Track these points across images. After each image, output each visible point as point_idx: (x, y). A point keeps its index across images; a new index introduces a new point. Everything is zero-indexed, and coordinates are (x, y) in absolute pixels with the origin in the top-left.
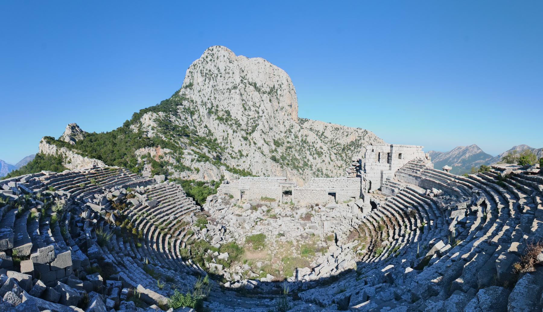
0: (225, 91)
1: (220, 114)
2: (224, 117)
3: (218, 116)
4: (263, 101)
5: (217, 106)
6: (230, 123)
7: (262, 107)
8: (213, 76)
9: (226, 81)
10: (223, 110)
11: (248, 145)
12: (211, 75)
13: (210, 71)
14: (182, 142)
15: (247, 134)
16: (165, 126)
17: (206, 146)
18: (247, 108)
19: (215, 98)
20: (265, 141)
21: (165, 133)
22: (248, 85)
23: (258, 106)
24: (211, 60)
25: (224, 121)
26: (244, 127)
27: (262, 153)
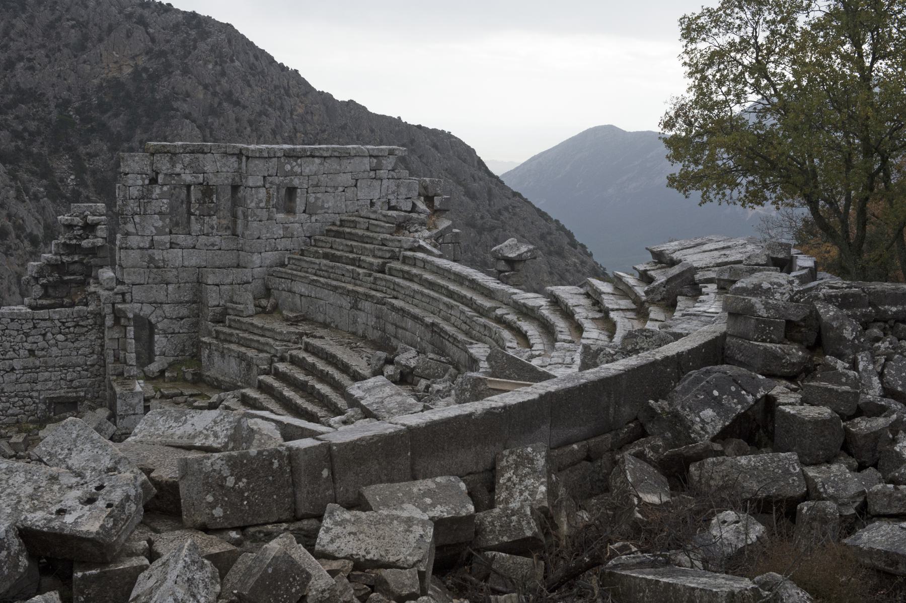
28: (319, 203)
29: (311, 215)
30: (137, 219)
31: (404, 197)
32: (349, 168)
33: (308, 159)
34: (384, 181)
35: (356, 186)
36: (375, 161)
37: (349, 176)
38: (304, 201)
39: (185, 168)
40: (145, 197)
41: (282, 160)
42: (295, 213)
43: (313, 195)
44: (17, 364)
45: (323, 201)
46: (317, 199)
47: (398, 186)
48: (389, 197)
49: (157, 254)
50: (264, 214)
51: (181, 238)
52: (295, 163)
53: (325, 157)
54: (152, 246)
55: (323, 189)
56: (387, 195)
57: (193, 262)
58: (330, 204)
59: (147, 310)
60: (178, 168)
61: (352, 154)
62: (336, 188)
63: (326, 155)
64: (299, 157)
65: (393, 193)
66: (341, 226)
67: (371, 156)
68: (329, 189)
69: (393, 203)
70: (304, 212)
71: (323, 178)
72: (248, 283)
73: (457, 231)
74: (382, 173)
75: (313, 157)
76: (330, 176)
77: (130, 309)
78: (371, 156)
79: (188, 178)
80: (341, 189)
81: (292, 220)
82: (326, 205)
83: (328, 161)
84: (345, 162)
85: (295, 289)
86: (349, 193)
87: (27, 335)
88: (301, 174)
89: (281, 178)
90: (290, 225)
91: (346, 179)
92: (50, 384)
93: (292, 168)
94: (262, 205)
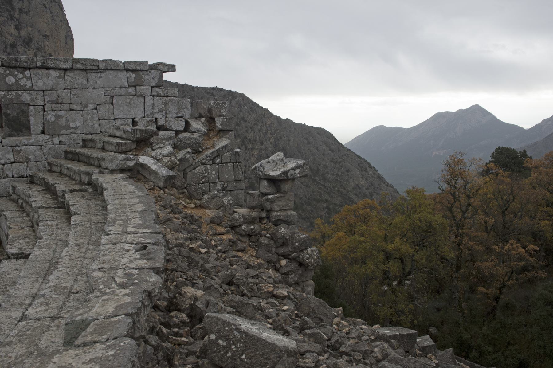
28: (62, 122)
29: (52, 136)
31: (174, 116)
32: (100, 83)
33: (39, 71)
34: (149, 99)
35: (112, 104)
36: (133, 75)
37: (101, 91)
38: (40, 120)
42: (30, 134)
43: (53, 113)
45: (67, 120)
46: (58, 117)
47: (166, 104)
48: (156, 116)
52: (20, 76)
53: (65, 70)
55: (66, 107)
56: (153, 113)
58: (78, 124)
61: (102, 67)
62: (85, 105)
63: (63, 66)
64: (26, 69)
65: (160, 111)
66: (84, 146)
67: (127, 70)
68: (75, 107)
69: (161, 122)
70: (43, 132)
71: (63, 94)
73: (238, 150)
74: (145, 89)
75: (48, 68)
76: (75, 92)
78: (127, 70)
80: (91, 107)
81: (26, 142)
82: (72, 125)
83: (71, 74)
84: (93, 76)
86: (103, 111)
88: (32, 88)
90: (23, 148)
91: (99, 95)
93: (18, 81)
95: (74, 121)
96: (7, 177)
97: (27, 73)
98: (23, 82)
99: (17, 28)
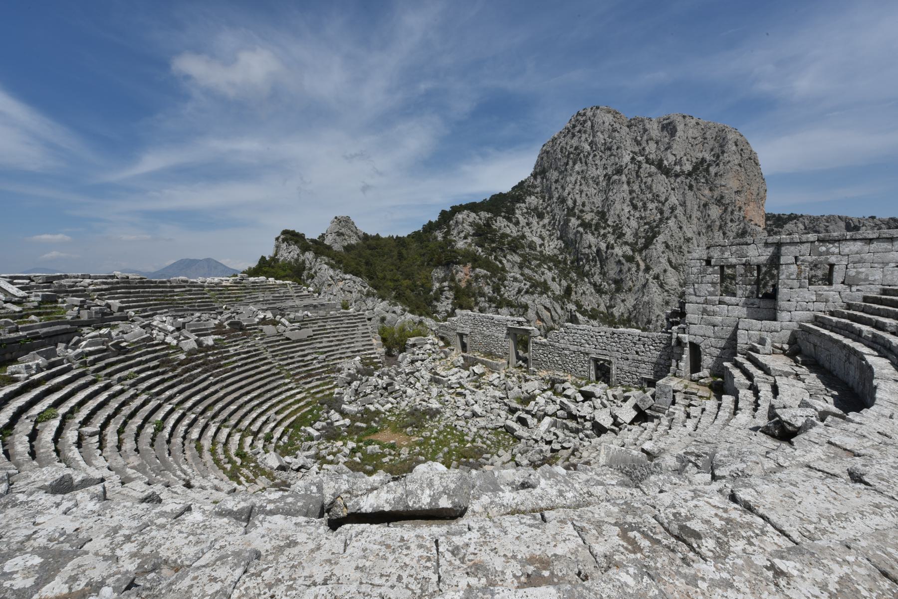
0: (601, 179)
1: (588, 217)
2: (594, 222)
3: (583, 220)
4: (673, 189)
5: (584, 205)
6: (602, 232)
7: (673, 200)
8: (582, 155)
9: (604, 161)
10: (592, 211)
11: (634, 269)
12: (579, 154)
13: (576, 148)
14: (508, 261)
15: (633, 251)
16: (483, 233)
17: (550, 269)
18: (640, 204)
19: (581, 192)
20: (670, 262)
21: (481, 246)
22: (644, 165)
23: (663, 199)
24: (580, 131)
25: (593, 228)
26: (629, 237)
27: (661, 286)
29: (850, 286)
30: (696, 286)
39: (732, 254)
40: (703, 272)
41: (816, 243)
44: (630, 357)
46: (858, 273)
49: (710, 308)
50: (796, 283)
51: (727, 299)
54: (706, 302)
57: (736, 314)
58: (877, 277)
59: (698, 340)
60: (726, 256)
71: (866, 256)
72: (777, 332)
77: (686, 338)
79: (733, 260)
85: (811, 340)
87: (635, 344)
89: (814, 257)
92: (645, 371)
94: (794, 277)
95: (873, 276)
96: (809, 310)
97: (836, 244)
98: (831, 250)
99: (711, 189)
